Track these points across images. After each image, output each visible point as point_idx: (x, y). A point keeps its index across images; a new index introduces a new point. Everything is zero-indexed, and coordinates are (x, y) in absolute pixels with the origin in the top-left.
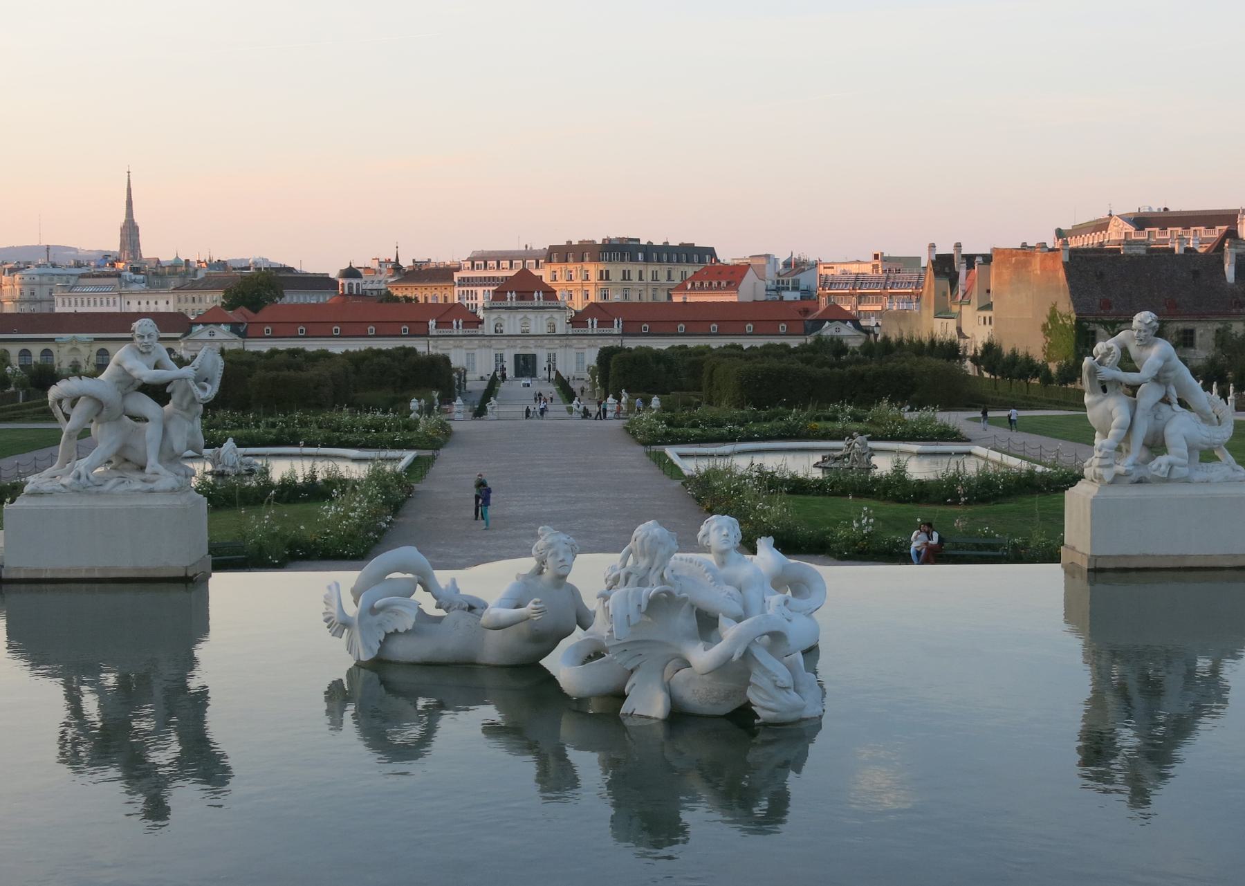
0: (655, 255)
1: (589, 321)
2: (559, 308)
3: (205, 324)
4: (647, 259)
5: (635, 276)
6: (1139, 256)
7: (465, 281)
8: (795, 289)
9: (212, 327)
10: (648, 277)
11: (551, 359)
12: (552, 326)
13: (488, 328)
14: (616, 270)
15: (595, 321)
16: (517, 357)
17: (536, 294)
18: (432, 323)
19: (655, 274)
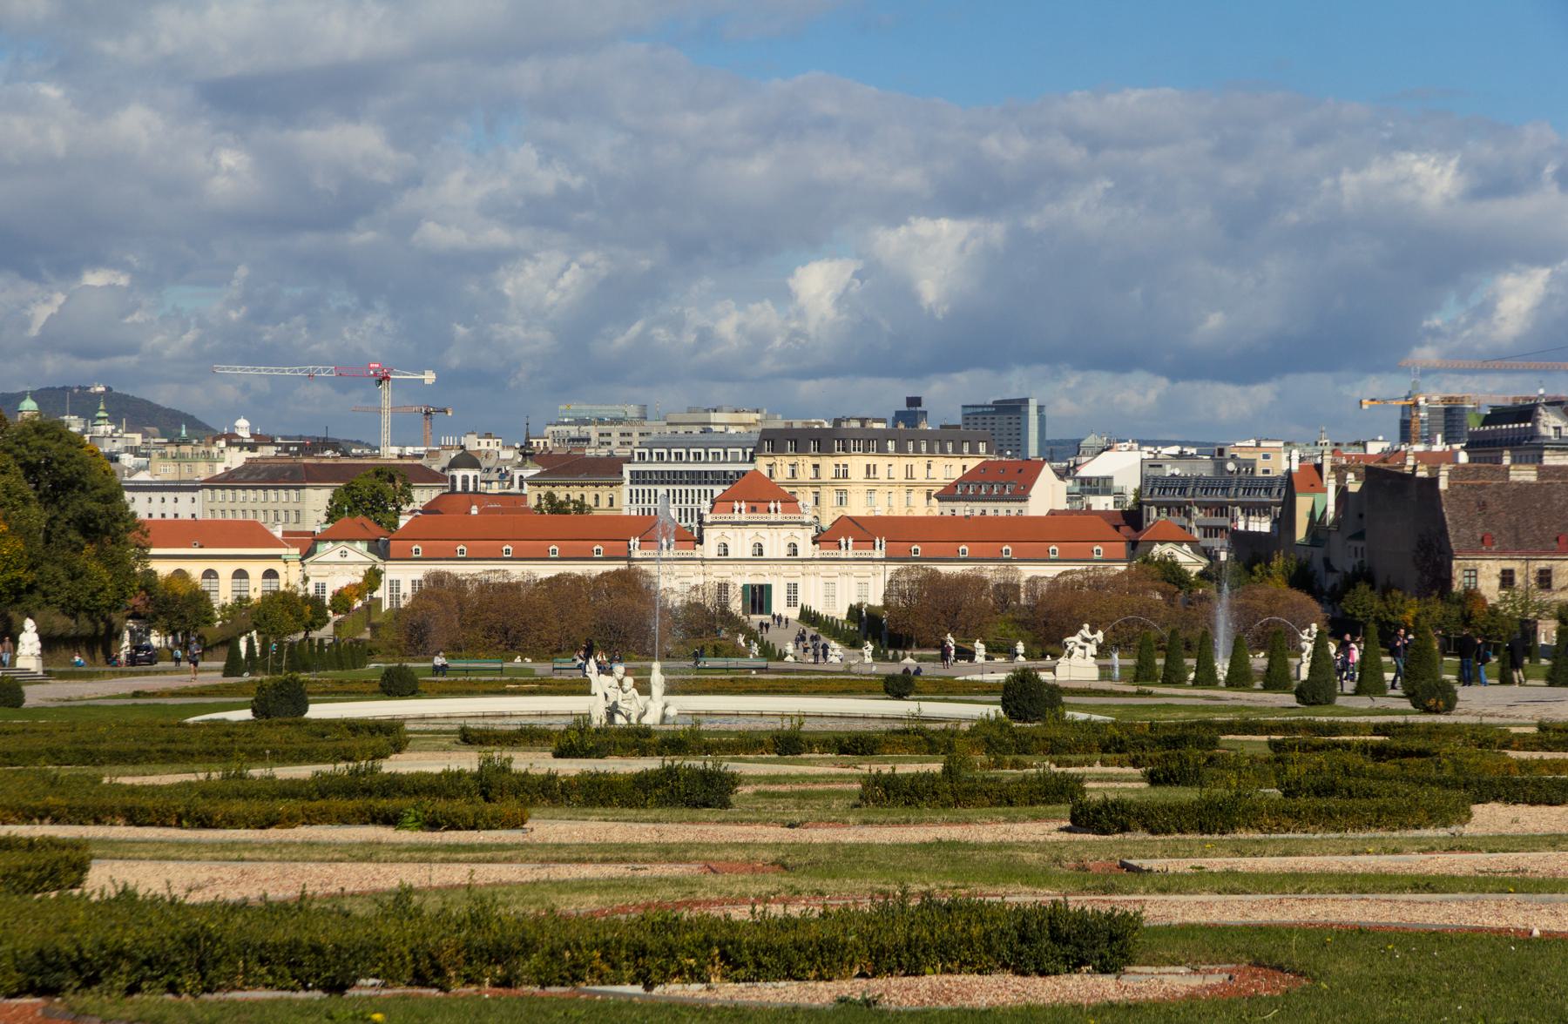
1: (843, 541)
2: (802, 524)
3: (334, 541)
5: (882, 473)
6: (1528, 484)
7: (637, 478)
8: (1107, 491)
9: (342, 546)
10: (899, 473)
11: (793, 590)
12: (794, 549)
13: (710, 548)
14: (857, 464)
15: (850, 541)
16: (745, 587)
17: (772, 505)
18: (634, 541)
19: (909, 470)
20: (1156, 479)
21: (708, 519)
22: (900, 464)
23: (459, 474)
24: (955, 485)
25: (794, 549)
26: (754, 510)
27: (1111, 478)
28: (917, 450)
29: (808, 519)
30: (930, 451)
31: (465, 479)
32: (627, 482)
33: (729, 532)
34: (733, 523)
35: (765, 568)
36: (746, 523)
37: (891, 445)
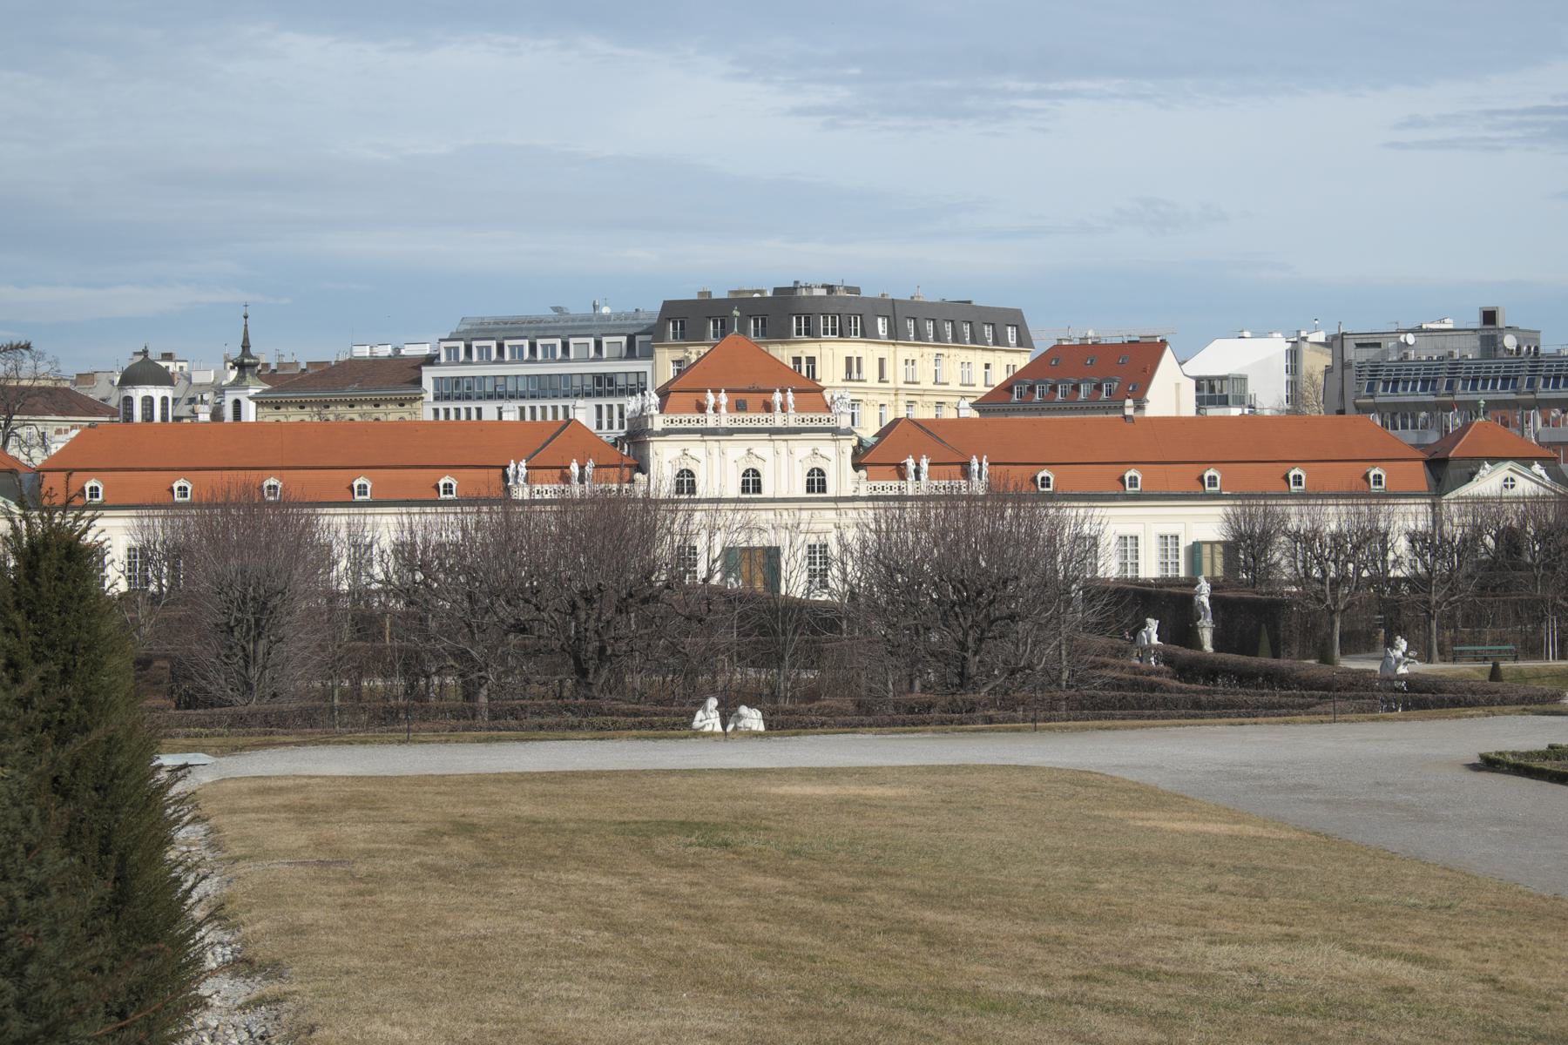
0: (910, 324)
1: (910, 463)
4: (895, 335)
5: (870, 371)
17: (777, 397)
20: (1375, 369)
21: (658, 423)
22: (897, 356)
23: (138, 393)
24: (1007, 387)
25: (816, 481)
26: (740, 407)
27: (1242, 380)
28: (920, 336)
29: (844, 422)
30: (938, 337)
31: (148, 402)
32: (429, 396)
33: (696, 448)
34: (705, 432)
35: (764, 517)
36: (730, 432)
37: (881, 326)
